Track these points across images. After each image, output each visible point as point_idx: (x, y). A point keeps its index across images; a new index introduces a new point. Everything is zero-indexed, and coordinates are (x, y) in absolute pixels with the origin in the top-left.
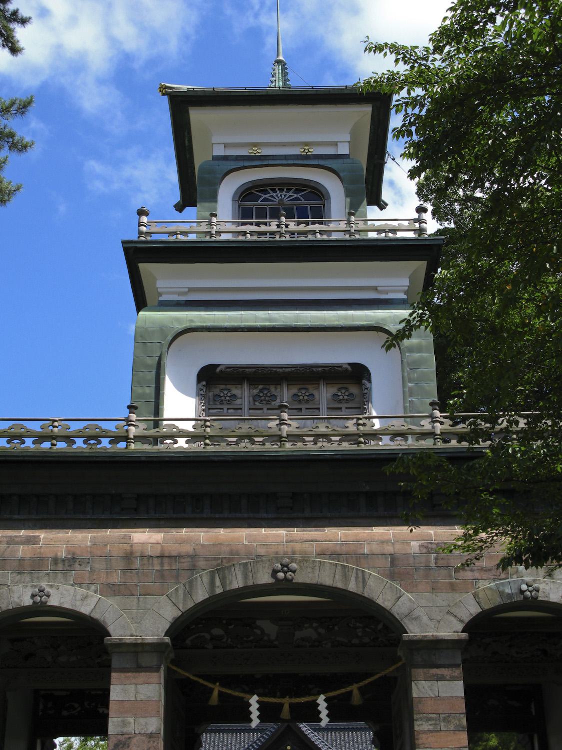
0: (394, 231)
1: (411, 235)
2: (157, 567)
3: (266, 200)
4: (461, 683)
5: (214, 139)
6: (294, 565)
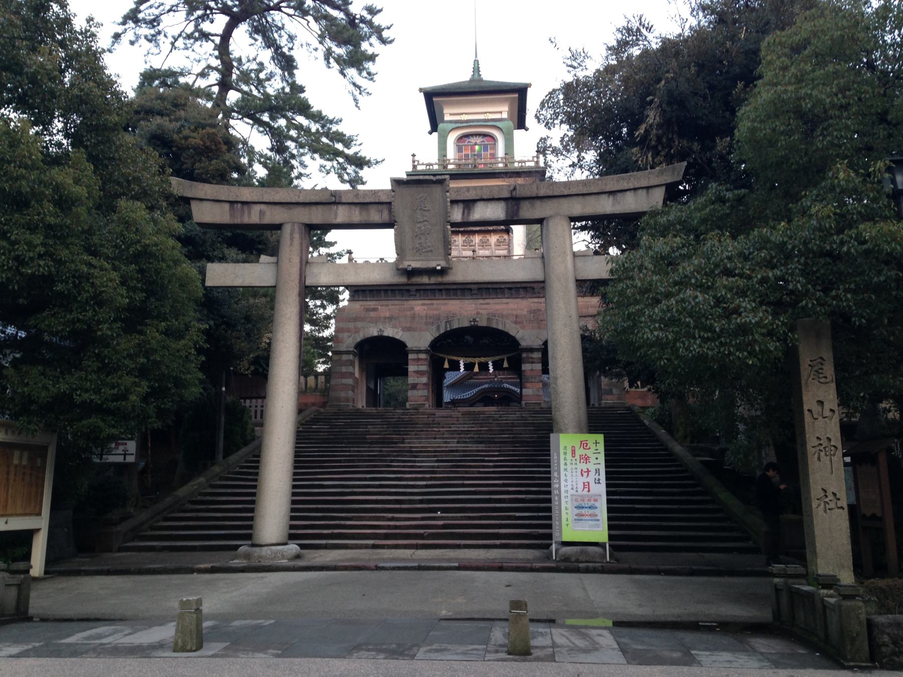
0: (525, 162)
1: (532, 164)
2: (424, 320)
3: (469, 142)
4: (541, 365)
5: (445, 111)
6: (477, 319)
